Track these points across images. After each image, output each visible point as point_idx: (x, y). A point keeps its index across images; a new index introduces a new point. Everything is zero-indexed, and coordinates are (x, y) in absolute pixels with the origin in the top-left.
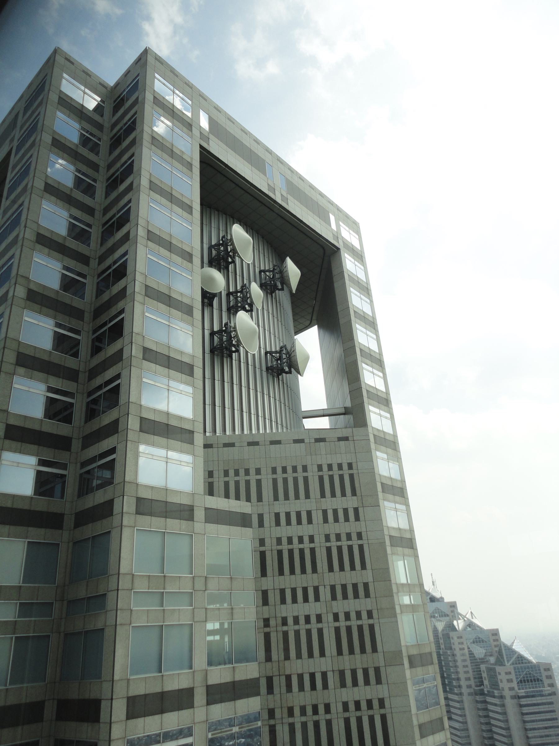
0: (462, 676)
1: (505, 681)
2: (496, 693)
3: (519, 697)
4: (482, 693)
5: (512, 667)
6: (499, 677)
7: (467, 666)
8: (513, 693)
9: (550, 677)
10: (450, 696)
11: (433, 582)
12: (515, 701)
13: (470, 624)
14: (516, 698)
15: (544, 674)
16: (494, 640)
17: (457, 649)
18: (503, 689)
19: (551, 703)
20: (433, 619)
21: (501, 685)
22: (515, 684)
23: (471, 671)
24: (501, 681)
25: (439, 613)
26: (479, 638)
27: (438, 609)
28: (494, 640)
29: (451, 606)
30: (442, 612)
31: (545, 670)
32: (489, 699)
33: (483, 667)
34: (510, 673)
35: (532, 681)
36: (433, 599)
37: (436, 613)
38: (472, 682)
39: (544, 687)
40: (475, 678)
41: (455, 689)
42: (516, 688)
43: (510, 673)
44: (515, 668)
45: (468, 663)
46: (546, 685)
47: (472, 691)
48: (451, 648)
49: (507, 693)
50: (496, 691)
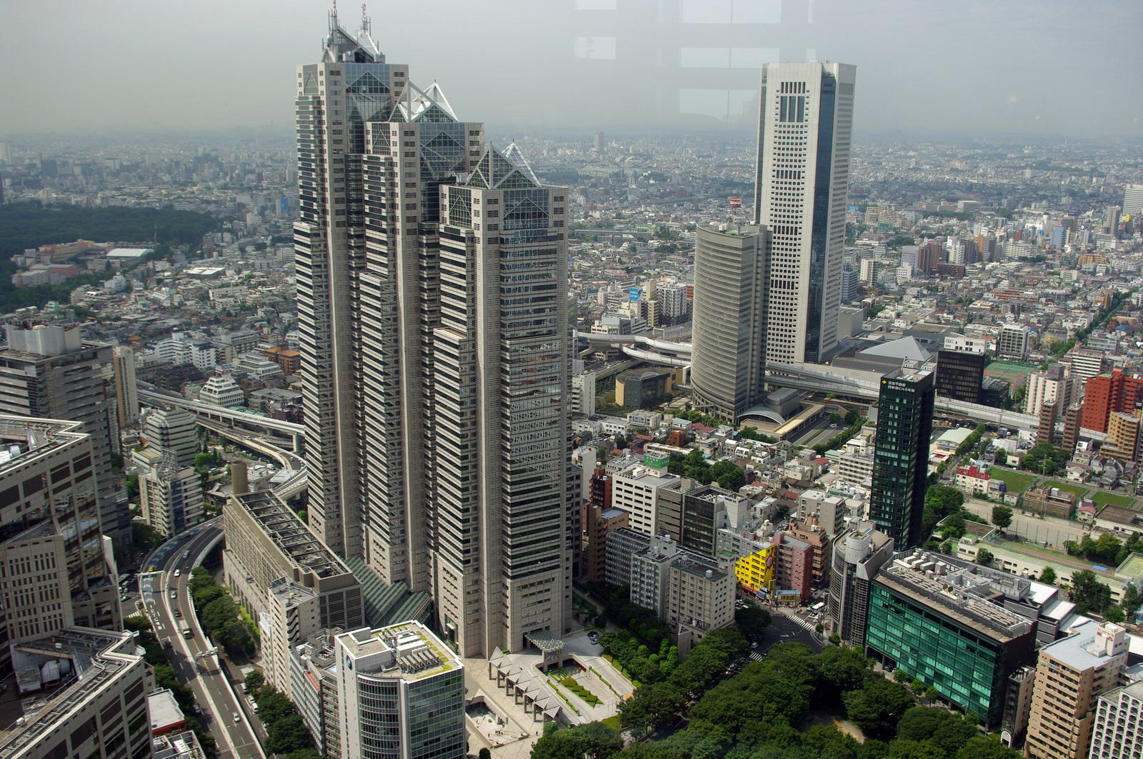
2: (463, 232)
5: (502, 191)
7: (414, 185)
8: (494, 234)
9: (559, 211)
10: (369, 233)
11: (365, 23)
12: (495, 247)
13: (434, 113)
14: (496, 243)
15: (552, 205)
19: (554, 252)
20: (351, 94)
23: (419, 194)
25: (370, 85)
26: (445, 137)
27: (370, 78)
30: (376, 83)
31: (556, 199)
32: (444, 242)
33: (445, 189)
34: (496, 201)
35: (523, 217)
36: (361, 57)
37: (365, 84)
39: (546, 226)
41: (384, 223)
43: (496, 201)
45: (417, 179)
46: (551, 223)
47: (415, 226)
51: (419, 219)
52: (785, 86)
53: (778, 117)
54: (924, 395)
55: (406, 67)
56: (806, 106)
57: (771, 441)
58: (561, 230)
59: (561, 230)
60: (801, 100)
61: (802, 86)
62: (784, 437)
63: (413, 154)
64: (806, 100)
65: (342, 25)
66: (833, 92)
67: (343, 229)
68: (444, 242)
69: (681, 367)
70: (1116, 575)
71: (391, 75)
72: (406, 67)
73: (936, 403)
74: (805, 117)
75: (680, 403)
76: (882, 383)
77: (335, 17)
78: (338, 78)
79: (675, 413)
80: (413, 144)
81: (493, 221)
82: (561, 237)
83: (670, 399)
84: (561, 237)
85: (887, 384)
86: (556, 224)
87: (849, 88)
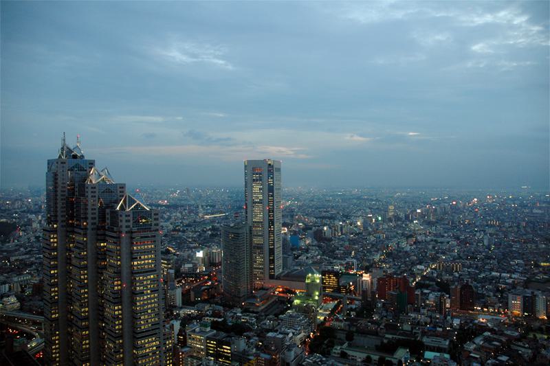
0: (90, 216)
1: (124, 221)
3: (132, 232)
4: (103, 228)
6: (120, 218)
12: (129, 235)
16: (120, 192)
17: (90, 196)
18: (121, 226)
19: (154, 236)
21: (120, 224)
22: (131, 224)
24: (121, 221)
28: (120, 192)
29: (90, 164)
32: (107, 233)
33: (108, 211)
36: (75, 157)
38: (96, 221)
40: (99, 218)
42: (131, 226)
43: (129, 216)
44: (133, 213)
47: (95, 226)
48: (84, 195)
49: (124, 229)
50: (115, 228)
51: (97, 223)
55: (94, 161)
57: (257, 313)
58: (157, 227)
59: (157, 227)
62: (262, 310)
63: (95, 196)
65: (67, 143)
67: (65, 228)
68: (107, 233)
70: (395, 357)
71: (88, 164)
72: (94, 161)
77: (64, 140)
78: (64, 165)
79: (217, 304)
80: (95, 192)
81: (129, 224)
82: (157, 230)
84: (157, 230)
86: (155, 225)
87: (279, 170)
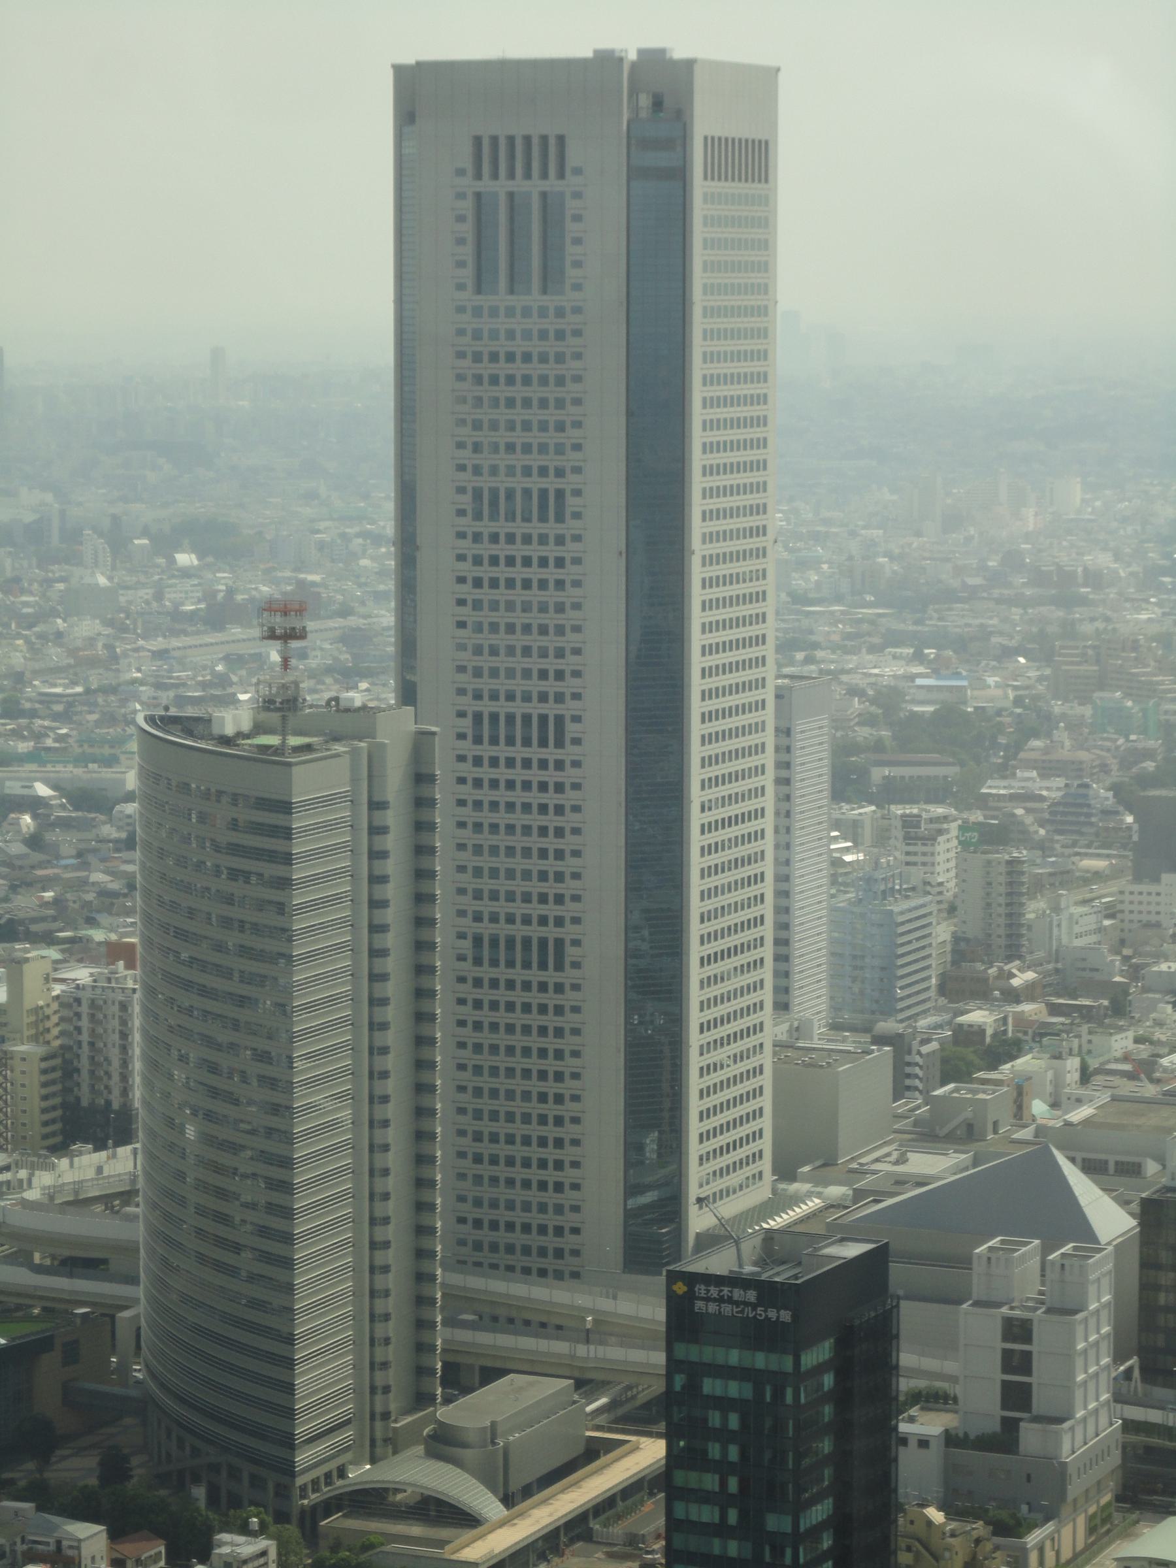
52: (489, 154)
53: (468, 273)
54: (846, 1339)
56: (572, 228)
60: (551, 208)
61: (549, 154)
64: (572, 206)
66: (680, 175)
69: (105, 1316)
73: (907, 1358)
74: (571, 273)
75: (77, 1468)
76: (671, 1297)
83: (41, 1441)
85: (691, 1296)
87: (751, 160)
